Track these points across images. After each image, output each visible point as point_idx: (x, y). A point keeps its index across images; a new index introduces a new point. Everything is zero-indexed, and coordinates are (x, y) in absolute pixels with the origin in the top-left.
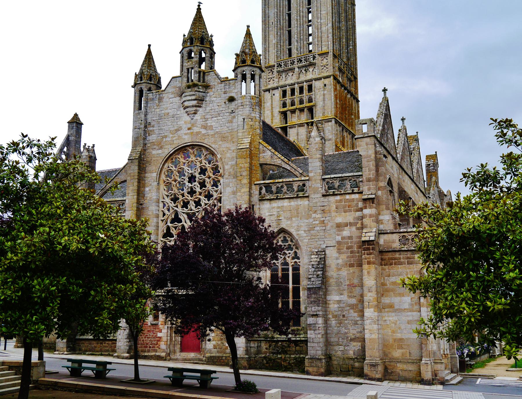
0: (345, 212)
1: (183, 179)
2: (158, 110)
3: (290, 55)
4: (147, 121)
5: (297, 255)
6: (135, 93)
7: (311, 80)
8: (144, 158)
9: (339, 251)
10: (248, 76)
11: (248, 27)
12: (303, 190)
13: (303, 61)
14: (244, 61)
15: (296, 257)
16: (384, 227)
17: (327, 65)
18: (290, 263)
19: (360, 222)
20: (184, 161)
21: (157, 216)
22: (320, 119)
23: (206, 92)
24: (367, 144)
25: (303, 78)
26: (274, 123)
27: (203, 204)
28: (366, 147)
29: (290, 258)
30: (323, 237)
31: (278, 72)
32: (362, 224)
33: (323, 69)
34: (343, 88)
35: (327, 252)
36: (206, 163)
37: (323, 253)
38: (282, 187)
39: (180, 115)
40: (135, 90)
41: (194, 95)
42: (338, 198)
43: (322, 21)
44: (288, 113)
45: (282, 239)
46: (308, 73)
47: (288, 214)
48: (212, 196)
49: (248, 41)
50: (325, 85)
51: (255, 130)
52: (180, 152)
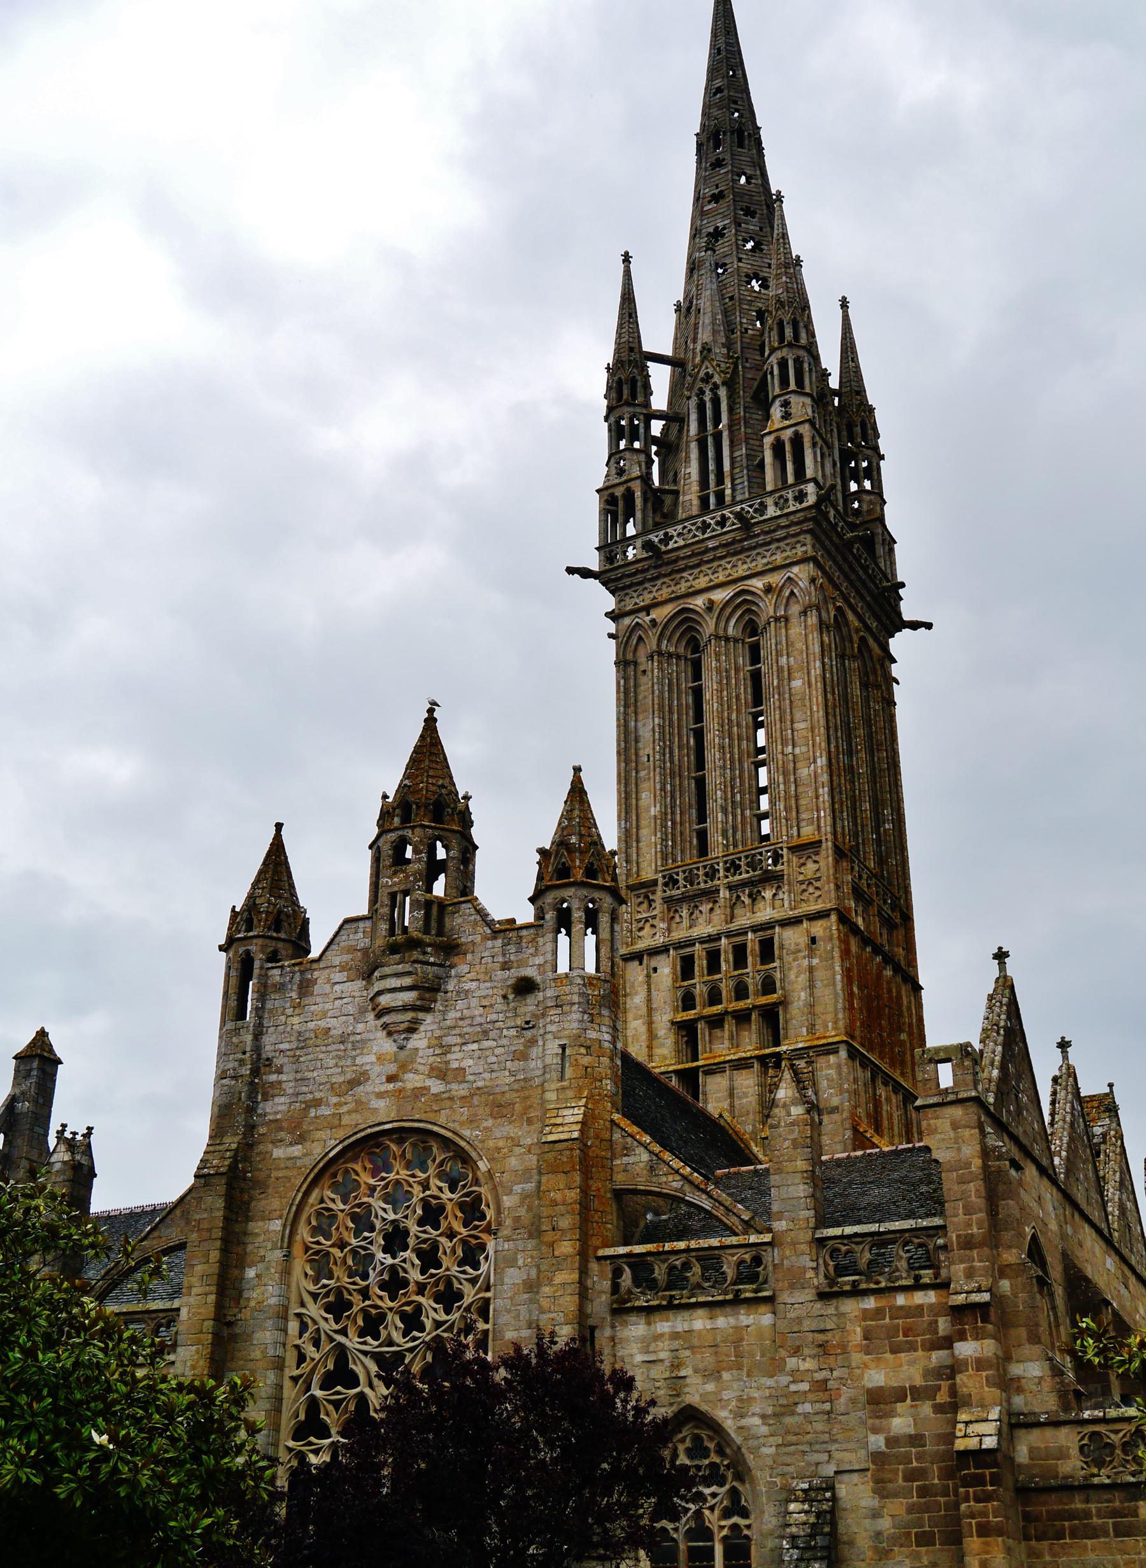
0: (893, 1352)
1: (365, 1238)
2: (296, 1020)
3: (703, 850)
4: (259, 1055)
5: (739, 1501)
6: (228, 968)
7: (769, 926)
9: (882, 1489)
10: (578, 915)
11: (577, 770)
12: (753, 1278)
13: (744, 868)
14: (564, 872)
15: (735, 1507)
16: (1026, 1404)
17: (818, 879)
18: (716, 1530)
19: (945, 1385)
20: (372, 1181)
21: (279, 1365)
22: (800, 1045)
23: (448, 963)
24: (955, 1126)
25: (744, 919)
26: (656, 1058)
27: (428, 1324)
28: (952, 1134)
29: (716, 1512)
30: (826, 1437)
31: (668, 901)
32: (953, 1391)
33: (804, 891)
34: (869, 949)
35: (842, 1490)
36: (440, 1189)
37: (828, 1495)
38: (686, 1266)
39: (363, 1036)
40: (229, 960)
41: (409, 973)
42: (870, 1303)
43: (797, 751)
44: (700, 1026)
45: (688, 1443)
46: (760, 905)
47: (707, 1359)
48: (460, 1296)
49: (576, 812)
50: (813, 940)
51: (598, 1084)
52: (361, 1151)
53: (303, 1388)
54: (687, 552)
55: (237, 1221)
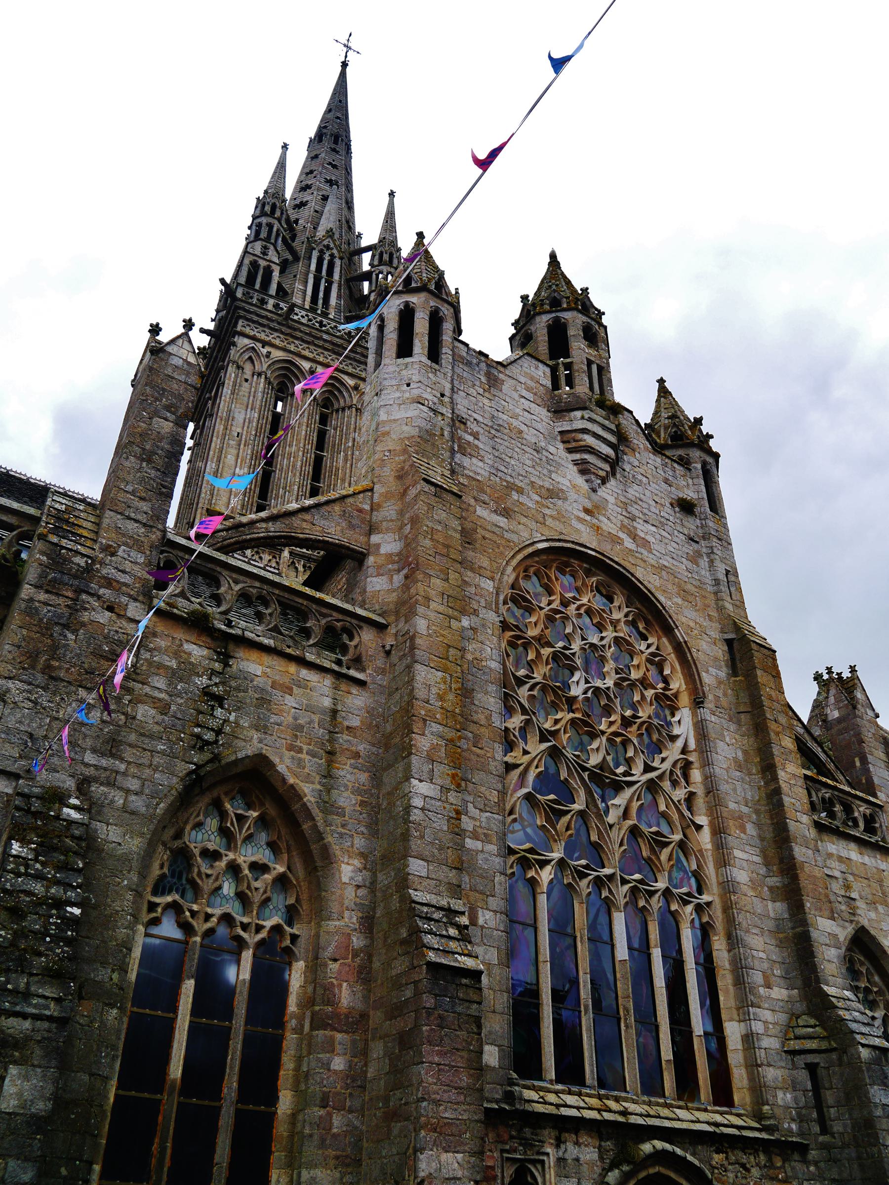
11: (661, 381)
52: (553, 561)
54: (307, 330)
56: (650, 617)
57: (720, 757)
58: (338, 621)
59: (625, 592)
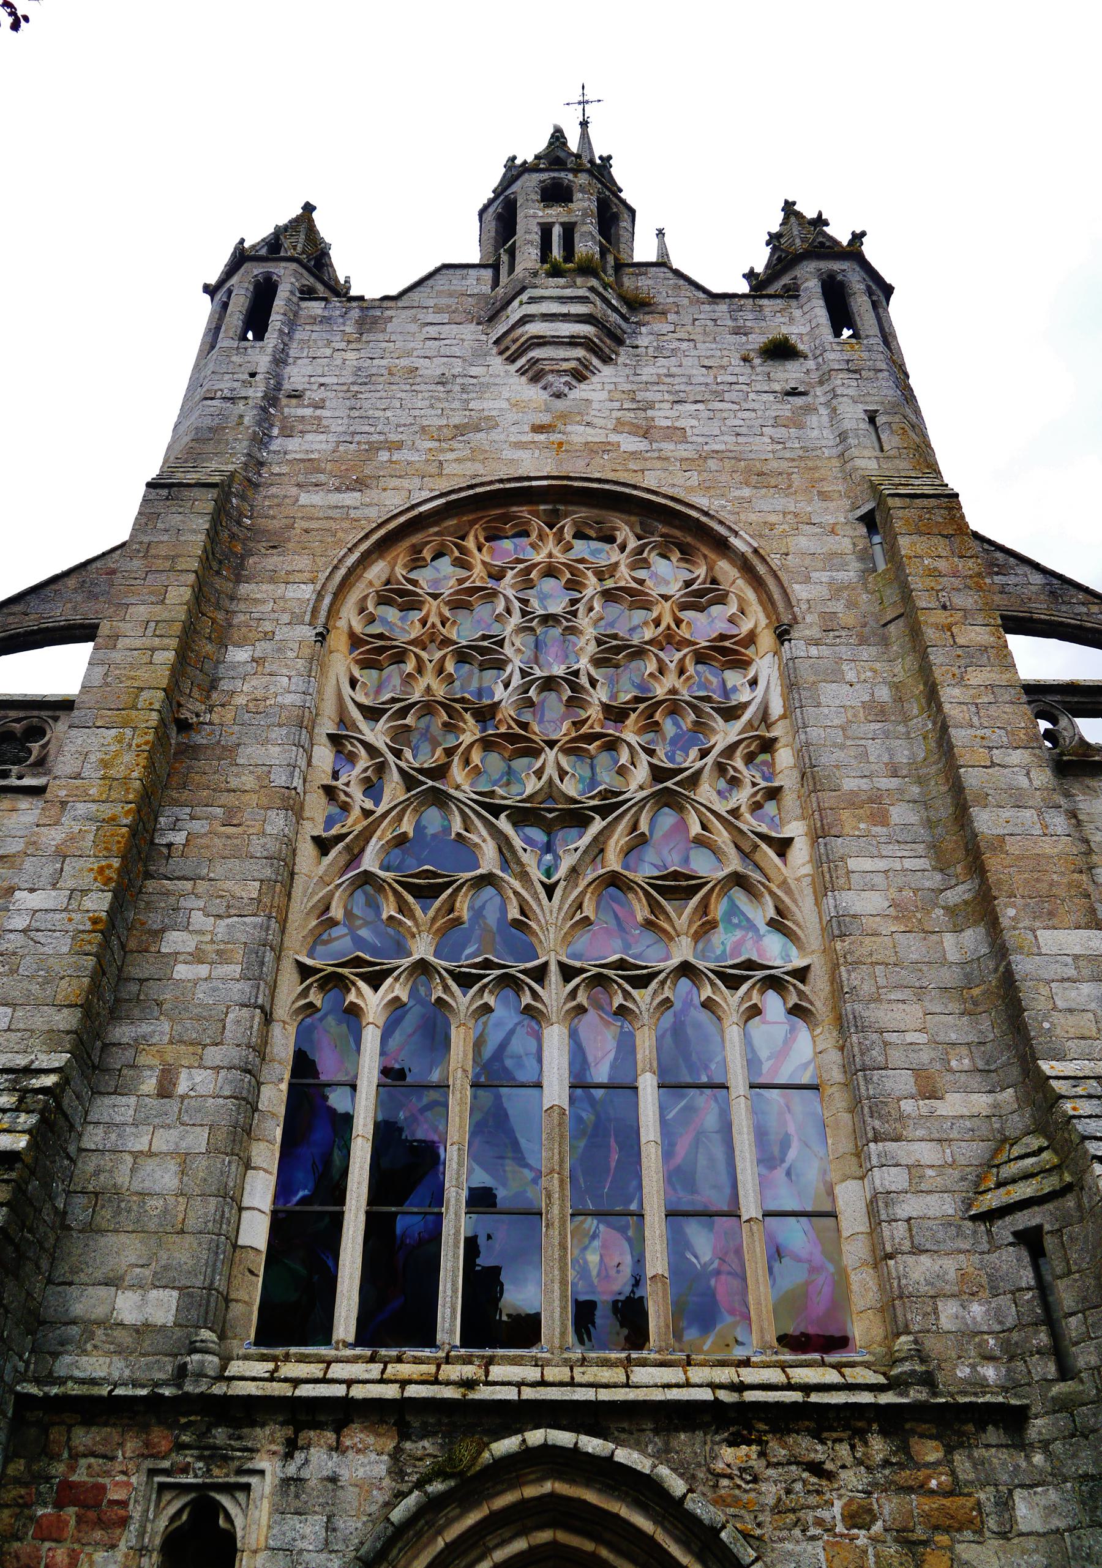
8: (241, 515)
21: (294, 808)
23: (633, 319)
39: (482, 380)
52: (472, 523)
53: (346, 857)
55: (218, 573)
56: (689, 539)
57: (826, 711)
58: (18, 720)
59: (633, 519)
